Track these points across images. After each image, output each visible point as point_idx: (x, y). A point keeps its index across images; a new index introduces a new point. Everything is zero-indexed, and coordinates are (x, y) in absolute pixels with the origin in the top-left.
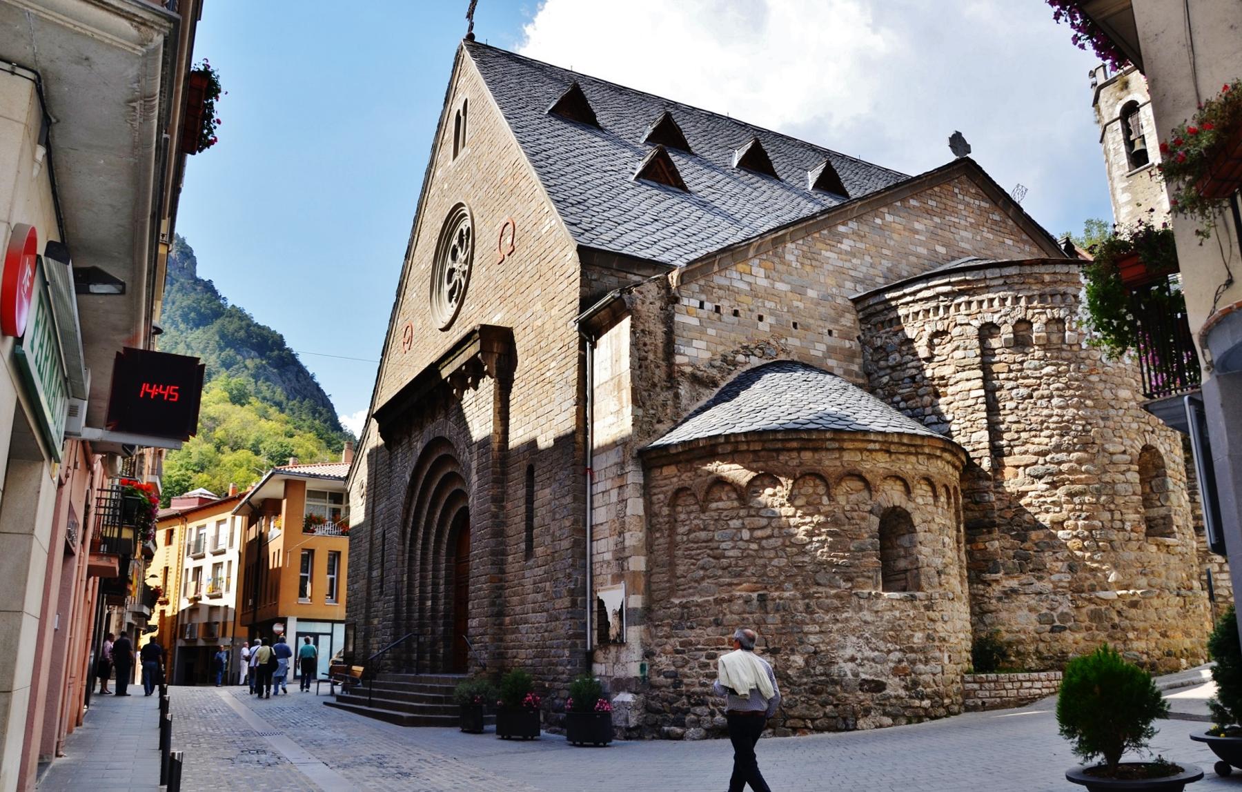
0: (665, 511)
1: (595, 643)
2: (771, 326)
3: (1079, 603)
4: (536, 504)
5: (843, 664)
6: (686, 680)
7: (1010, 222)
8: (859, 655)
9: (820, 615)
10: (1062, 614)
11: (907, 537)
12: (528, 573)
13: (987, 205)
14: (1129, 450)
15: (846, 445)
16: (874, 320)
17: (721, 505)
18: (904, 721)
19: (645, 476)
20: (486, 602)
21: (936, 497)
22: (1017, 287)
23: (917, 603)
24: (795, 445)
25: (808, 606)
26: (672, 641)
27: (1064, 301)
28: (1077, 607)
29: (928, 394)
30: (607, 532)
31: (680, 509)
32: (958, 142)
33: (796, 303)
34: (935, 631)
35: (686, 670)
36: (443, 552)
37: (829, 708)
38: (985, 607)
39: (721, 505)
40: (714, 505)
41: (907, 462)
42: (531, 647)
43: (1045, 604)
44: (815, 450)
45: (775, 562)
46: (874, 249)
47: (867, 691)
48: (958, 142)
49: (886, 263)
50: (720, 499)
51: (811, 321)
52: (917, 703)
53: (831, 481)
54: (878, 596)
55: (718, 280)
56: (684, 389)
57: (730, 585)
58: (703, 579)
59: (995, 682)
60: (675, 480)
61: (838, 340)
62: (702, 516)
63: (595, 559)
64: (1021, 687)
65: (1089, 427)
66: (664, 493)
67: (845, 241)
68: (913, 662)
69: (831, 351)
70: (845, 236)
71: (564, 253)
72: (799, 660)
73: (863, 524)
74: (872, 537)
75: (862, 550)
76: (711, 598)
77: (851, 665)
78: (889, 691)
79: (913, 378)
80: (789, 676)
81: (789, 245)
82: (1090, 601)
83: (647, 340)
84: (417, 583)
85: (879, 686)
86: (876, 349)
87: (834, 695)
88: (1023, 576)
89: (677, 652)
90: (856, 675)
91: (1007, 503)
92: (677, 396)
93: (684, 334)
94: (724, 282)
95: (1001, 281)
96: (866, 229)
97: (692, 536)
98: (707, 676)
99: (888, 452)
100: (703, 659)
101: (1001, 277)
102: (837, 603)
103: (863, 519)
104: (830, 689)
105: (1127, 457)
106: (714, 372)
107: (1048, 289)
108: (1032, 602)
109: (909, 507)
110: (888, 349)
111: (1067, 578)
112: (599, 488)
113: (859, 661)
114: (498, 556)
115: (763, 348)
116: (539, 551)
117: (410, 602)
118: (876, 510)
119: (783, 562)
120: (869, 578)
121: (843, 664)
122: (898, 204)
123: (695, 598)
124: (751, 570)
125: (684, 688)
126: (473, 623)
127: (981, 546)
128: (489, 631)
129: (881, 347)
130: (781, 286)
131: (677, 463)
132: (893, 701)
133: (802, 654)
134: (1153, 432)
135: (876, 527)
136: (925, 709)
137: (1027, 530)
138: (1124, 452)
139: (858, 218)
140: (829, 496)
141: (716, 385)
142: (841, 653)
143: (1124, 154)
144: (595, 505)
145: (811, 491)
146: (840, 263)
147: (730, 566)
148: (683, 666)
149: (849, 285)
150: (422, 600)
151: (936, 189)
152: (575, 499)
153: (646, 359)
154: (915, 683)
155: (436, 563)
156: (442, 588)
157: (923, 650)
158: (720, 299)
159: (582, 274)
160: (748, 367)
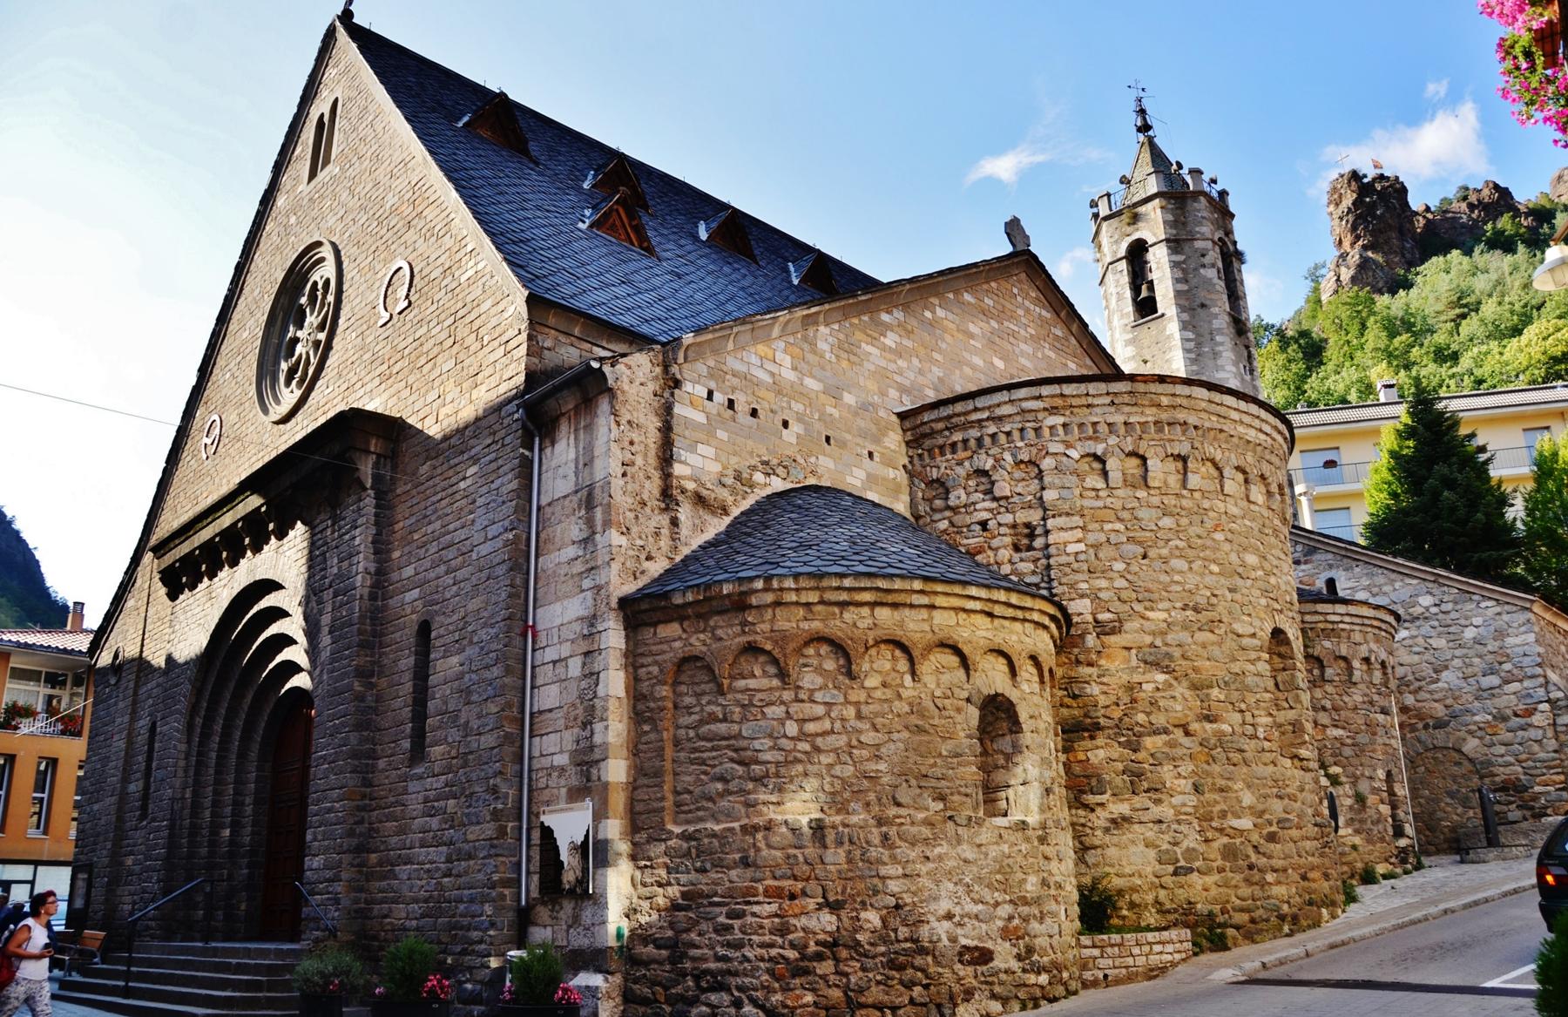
0: (664, 691)
1: (535, 894)
2: (798, 436)
3: (1210, 835)
4: (433, 680)
5: (935, 924)
7: (1073, 341)
8: (957, 910)
9: (903, 850)
10: (1188, 849)
11: (1008, 738)
12: (413, 786)
13: (1048, 315)
14: (1260, 634)
15: (940, 601)
16: (928, 443)
17: (752, 683)
18: (1016, 1006)
19: (627, 637)
20: (339, 830)
21: (1042, 682)
22: (1127, 409)
23: (1030, 833)
24: (867, 597)
25: (885, 837)
27: (1184, 433)
28: (1207, 841)
29: (1005, 547)
30: (562, 721)
31: (683, 688)
32: (1013, 228)
33: (830, 410)
34: (1051, 874)
35: (693, 936)
36: (253, 755)
37: (917, 990)
38: (1088, 841)
39: (752, 683)
40: (741, 683)
41: (1011, 632)
42: (416, 901)
43: (1167, 837)
44: (895, 606)
46: (922, 351)
47: (970, 963)
48: (1013, 228)
49: (937, 372)
51: (848, 437)
52: (1032, 979)
53: (916, 653)
54: (980, 823)
55: (733, 363)
56: (685, 513)
59: (1119, 945)
60: (677, 644)
61: (881, 467)
62: (721, 700)
63: (536, 765)
64: (1151, 952)
65: (1214, 601)
67: (889, 334)
68: (1026, 920)
69: (872, 479)
70: (888, 327)
71: (500, 307)
72: (872, 918)
73: (959, 718)
74: (970, 737)
75: (957, 755)
76: (736, 825)
77: (946, 924)
78: (997, 963)
79: (984, 525)
80: (858, 943)
81: (822, 328)
82: (1221, 830)
84: (207, 802)
85: (983, 956)
86: (930, 483)
87: (923, 971)
90: (953, 940)
91: (1114, 698)
92: (675, 522)
93: (687, 433)
94: (739, 367)
95: (1107, 400)
97: (704, 729)
98: (729, 945)
99: (990, 615)
100: (722, 919)
102: (926, 832)
103: (959, 710)
104: (918, 961)
105: (1256, 642)
106: (724, 494)
107: (1164, 416)
108: (1149, 834)
109: (1014, 695)
110: (950, 484)
111: (1192, 800)
112: (550, 654)
113: (957, 919)
114: (364, 761)
115: (787, 465)
116: (436, 751)
117: (194, 830)
118: (975, 699)
121: (935, 924)
122: (951, 296)
123: (709, 825)
125: (688, 965)
126: (314, 862)
127: (1081, 756)
128: (344, 875)
129: (938, 480)
130: (812, 384)
131: (681, 619)
132: (1003, 976)
135: (975, 722)
136: (1042, 987)
137: (1140, 735)
139: (906, 307)
140: (913, 673)
141: (725, 512)
142: (933, 907)
143: (1129, 301)
144: (539, 682)
145: (888, 666)
146: (883, 363)
148: (688, 930)
149: (893, 393)
150: (215, 828)
151: (993, 284)
152: (508, 671)
153: (633, 464)
154: (1030, 950)
155: (240, 770)
156: (249, 810)
157: (1037, 901)
158: (734, 389)
159: (530, 338)
160: (769, 491)
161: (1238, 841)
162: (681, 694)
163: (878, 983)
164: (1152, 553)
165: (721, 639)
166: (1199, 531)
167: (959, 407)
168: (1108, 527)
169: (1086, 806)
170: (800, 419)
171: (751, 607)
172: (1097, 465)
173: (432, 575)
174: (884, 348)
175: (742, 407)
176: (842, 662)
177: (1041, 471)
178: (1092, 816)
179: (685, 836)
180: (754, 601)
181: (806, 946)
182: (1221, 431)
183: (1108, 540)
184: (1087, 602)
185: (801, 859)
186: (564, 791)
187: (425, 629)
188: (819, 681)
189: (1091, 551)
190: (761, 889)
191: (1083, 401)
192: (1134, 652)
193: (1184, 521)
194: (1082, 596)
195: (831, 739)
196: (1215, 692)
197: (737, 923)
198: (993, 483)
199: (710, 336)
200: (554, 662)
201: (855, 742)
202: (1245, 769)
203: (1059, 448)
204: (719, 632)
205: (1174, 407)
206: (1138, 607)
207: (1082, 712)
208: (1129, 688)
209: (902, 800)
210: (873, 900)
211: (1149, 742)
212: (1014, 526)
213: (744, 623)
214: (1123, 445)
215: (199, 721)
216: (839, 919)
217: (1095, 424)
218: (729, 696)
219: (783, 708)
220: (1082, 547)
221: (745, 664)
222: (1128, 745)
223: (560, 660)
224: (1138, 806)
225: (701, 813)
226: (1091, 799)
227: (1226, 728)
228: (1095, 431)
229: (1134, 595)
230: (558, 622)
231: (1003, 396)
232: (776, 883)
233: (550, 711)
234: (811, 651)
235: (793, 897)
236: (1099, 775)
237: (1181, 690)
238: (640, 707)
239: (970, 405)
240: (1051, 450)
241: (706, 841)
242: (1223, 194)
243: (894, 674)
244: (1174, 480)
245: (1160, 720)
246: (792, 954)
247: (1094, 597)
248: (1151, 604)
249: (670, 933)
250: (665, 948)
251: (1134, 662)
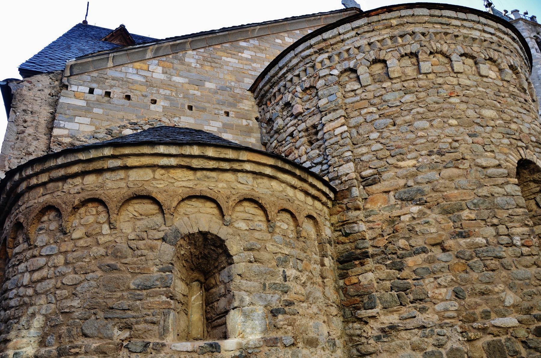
2: (164, 107)
3: (472, 335)
10: (452, 350)
14: (505, 164)
28: (469, 340)
29: (303, 145)
38: (363, 348)
43: (431, 341)
44: (99, 172)
51: (207, 105)
53: (112, 206)
65: (456, 144)
69: (226, 127)
73: (151, 255)
79: (291, 135)
81: (190, 52)
82: (484, 330)
83: (28, 118)
88: (404, 309)
91: (379, 231)
95: (353, 33)
96: (267, 45)
101: (353, 29)
107: (396, 32)
108: (415, 339)
109: (222, 232)
111: (454, 305)
118: (171, 238)
120: (154, 323)
127: (354, 280)
130: (177, 79)
134: (527, 148)
137: (402, 257)
138: (499, 166)
158: (111, 87)
161: (503, 338)
164: (399, 121)
166: (436, 99)
167: (272, 72)
168: (364, 111)
169: (360, 320)
170: (166, 98)
172: (353, 75)
174: (241, 59)
175: (117, 93)
178: (366, 328)
182: (446, 34)
183: (366, 121)
184: (351, 164)
189: (354, 131)
191: (338, 39)
192: (392, 193)
193: (422, 95)
194: (347, 162)
196: (465, 214)
199: (90, 59)
201: (59, 284)
202: (504, 273)
203: (326, 72)
205: (402, 25)
206: (391, 160)
207: (353, 245)
208: (392, 221)
209: (87, 332)
211: (410, 261)
212: (307, 130)
214: (368, 57)
217: (348, 51)
220: (345, 128)
222: (393, 266)
224: (405, 315)
226: (363, 313)
227: (480, 240)
228: (349, 55)
229: (388, 153)
231: (292, 54)
234: (45, 218)
236: (369, 294)
237: (433, 216)
239: (276, 68)
240: (321, 75)
242: (533, 18)
243: (96, 225)
244: (410, 71)
245: (418, 242)
247: (356, 160)
248: (402, 156)
251: (393, 201)
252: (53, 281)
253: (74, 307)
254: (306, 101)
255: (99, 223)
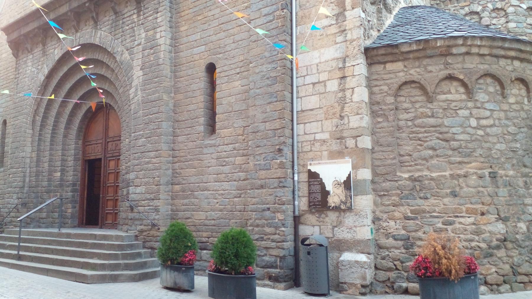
0: (390, 100)
6: (419, 243)
17: (449, 97)
26: (402, 209)
31: (402, 99)
39: (449, 97)
40: (443, 97)
44: (522, 60)
45: (498, 146)
50: (450, 92)
57: (460, 163)
58: (432, 157)
60: (401, 74)
62: (429, 105)
66: (388, 85)
72: (523, 226)
76: (447, 174)
80: (517, 240)
89: (407, 218)
97: (419, 121)
100: (440, 225)
119: (503, 147)
124: (479, 151)
133: (525, 222)
144: (301, 95)
147: (460, 147)
150: (51, 173)
156: (71, 163)
162: (401, 102)
163: (527, 261)
165: (431, 72)
171: (452, 54)
173: (214, 38)
176: (498, 88)
177: (506, 14)
179: (410, 179)
180: (455, 51)
181: (491, 241)
185: (486, 193)
186: (325, 153)
187: (211, 69)
188: (487, 98)
190: (464, 209)
195: (494, 129)
197: (449, 228)
198: (481, 18)
200: (314, 84)
204: (430, 68)
210: (522, 217)
213: (447, 64)
215: (39, 119)
216: (507, 226)
218: (435, 104)
219: (468, 111)
221: (445, 86)
223: (319, 82)
225: (419, 167)
230: (317, 61)
232: (474, 207)
233: (312, 110)
235: (483, 214)
238: (376, 108)
241: (427, 182)
243: (520, 98)
246: (483, 245)
249: (403, 232)
250: (401, 240)
252: (500, 129)
253: (518, 148)
254: (494, 18)
255: (521, 96)
